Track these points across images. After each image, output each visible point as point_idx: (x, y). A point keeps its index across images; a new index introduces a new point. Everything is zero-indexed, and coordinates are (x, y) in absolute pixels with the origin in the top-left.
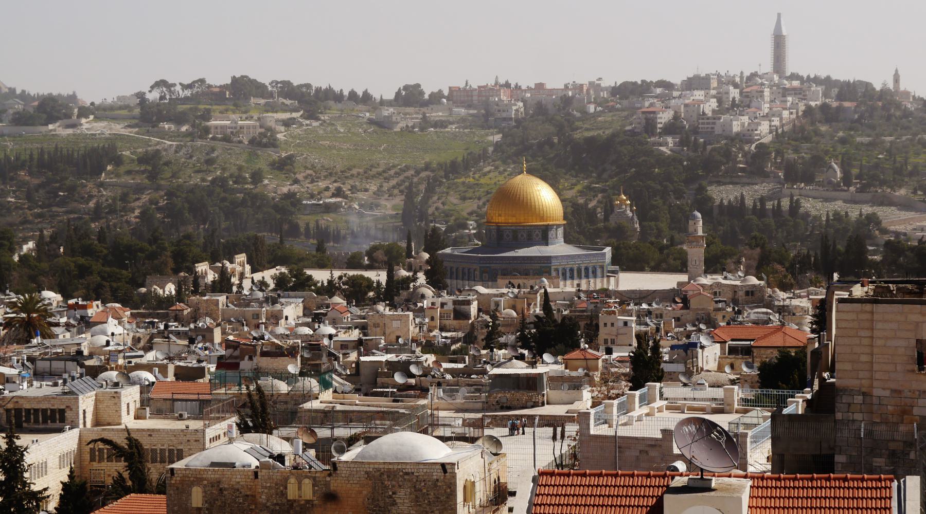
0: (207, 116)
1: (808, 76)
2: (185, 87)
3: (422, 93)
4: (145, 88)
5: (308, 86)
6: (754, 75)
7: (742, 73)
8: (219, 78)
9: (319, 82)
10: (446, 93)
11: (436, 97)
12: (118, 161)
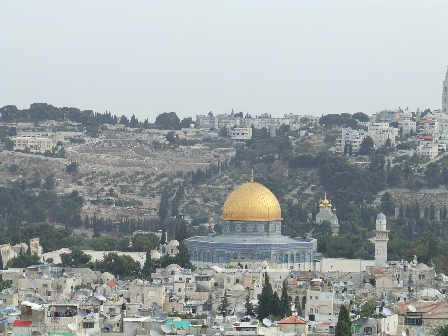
0: (13, 132)
3: (177, 119)
5: (90, 112)
6: (428, 111)
7: (418, 109)
10: (194, 119)
11: (187, 123)
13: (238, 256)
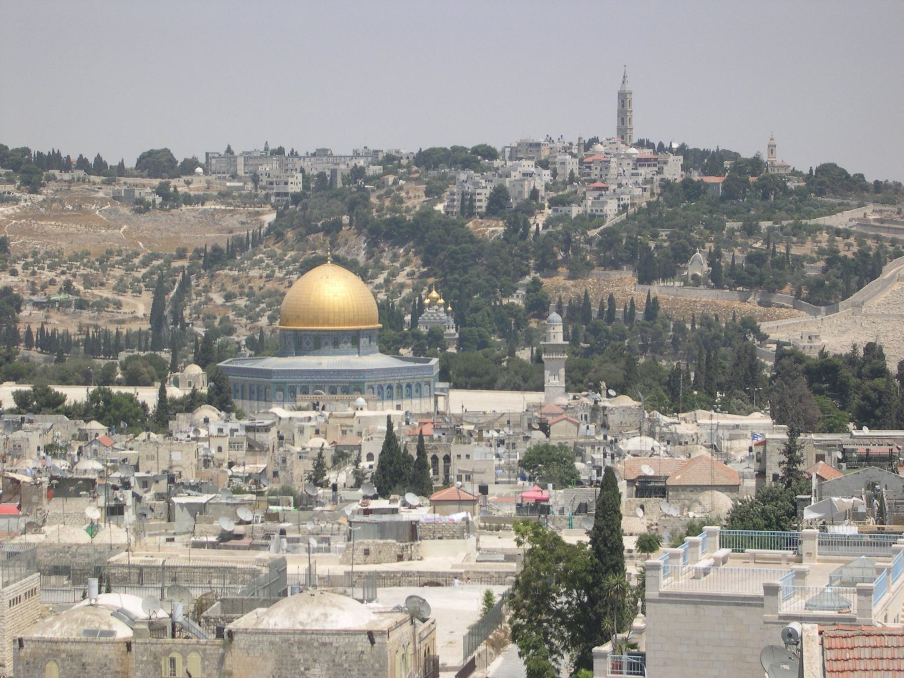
3: (172, 161)
5: (26, 151)
6: (595, 141)
9: (40, 145)
10: (202, 160)
11: (189, 167)
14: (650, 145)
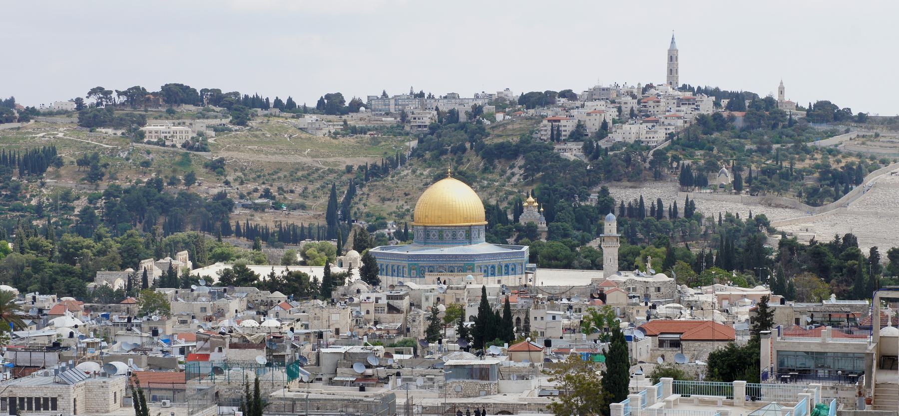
1: (699, 88)
2: (120, 94)
3: (343, 101)
4: (83, 95)
5: (236, 94)
6: (650, 86)
7: (639, 84)
8: (153, 86)
9: (247, 90)
10: (365, 101)
11: (356, 106)
12: (59, 163)
13: (154, 234)
14: (691, 89)
